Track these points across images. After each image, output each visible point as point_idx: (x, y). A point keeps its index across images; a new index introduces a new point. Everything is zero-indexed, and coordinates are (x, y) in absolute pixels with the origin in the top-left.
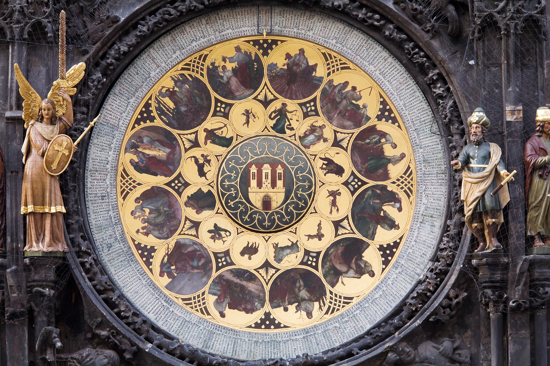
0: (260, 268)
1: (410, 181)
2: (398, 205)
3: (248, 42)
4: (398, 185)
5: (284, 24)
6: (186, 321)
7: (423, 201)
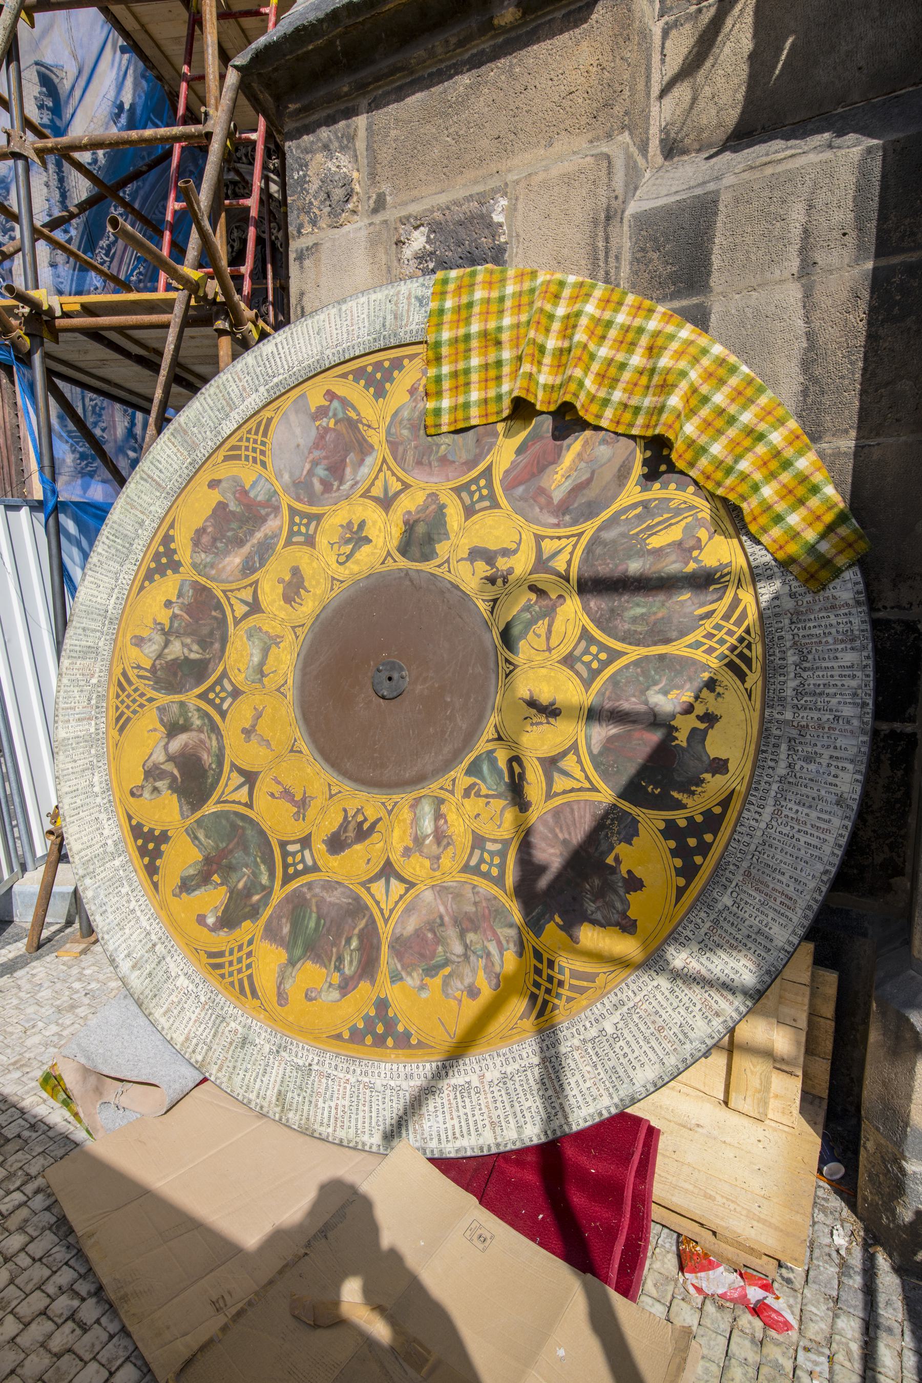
0: (255, 593)
1: (231, 979)
2: (211, 920)
3: (725, 803)
4: (240, 948)
5: (726, 926)
6: (232, 410)
7: (182, 978)
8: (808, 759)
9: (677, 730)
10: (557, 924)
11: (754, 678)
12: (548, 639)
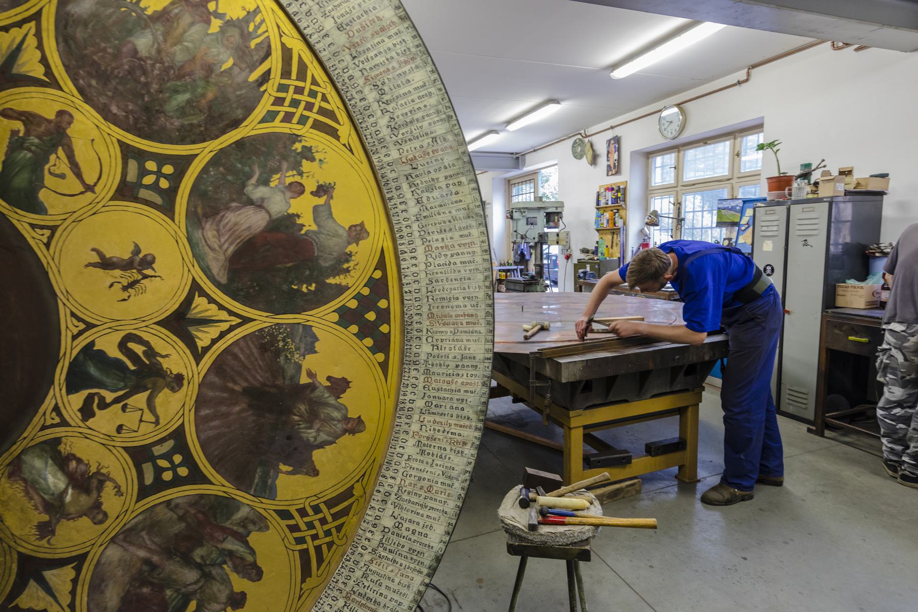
3: (381, 264)
5: (436, 369)
8: (430, 189)
9: (298, 216)
10: (288, 473)
11: (345, 129)
12: (79, 175)
